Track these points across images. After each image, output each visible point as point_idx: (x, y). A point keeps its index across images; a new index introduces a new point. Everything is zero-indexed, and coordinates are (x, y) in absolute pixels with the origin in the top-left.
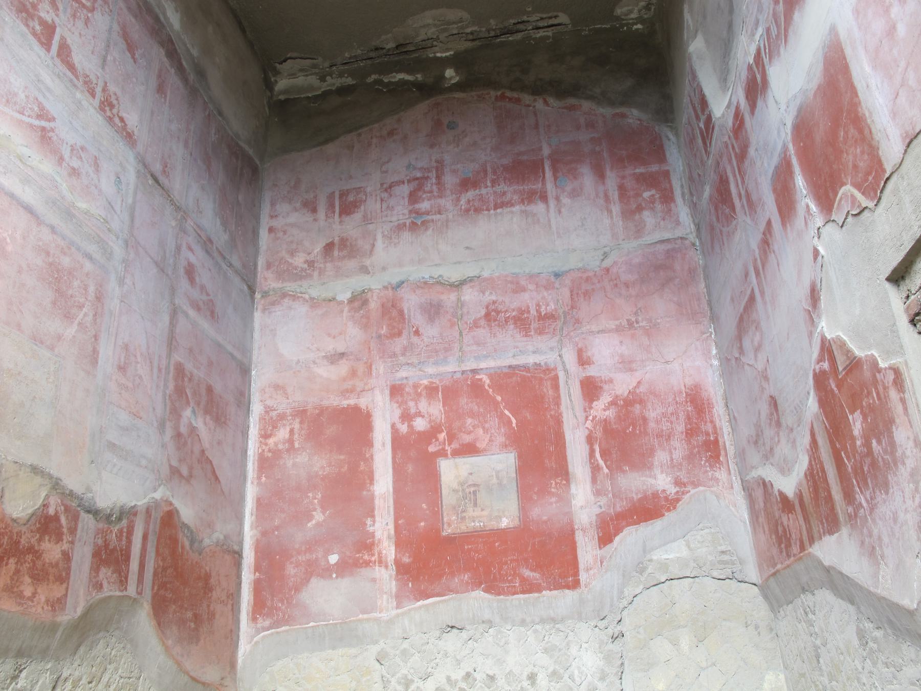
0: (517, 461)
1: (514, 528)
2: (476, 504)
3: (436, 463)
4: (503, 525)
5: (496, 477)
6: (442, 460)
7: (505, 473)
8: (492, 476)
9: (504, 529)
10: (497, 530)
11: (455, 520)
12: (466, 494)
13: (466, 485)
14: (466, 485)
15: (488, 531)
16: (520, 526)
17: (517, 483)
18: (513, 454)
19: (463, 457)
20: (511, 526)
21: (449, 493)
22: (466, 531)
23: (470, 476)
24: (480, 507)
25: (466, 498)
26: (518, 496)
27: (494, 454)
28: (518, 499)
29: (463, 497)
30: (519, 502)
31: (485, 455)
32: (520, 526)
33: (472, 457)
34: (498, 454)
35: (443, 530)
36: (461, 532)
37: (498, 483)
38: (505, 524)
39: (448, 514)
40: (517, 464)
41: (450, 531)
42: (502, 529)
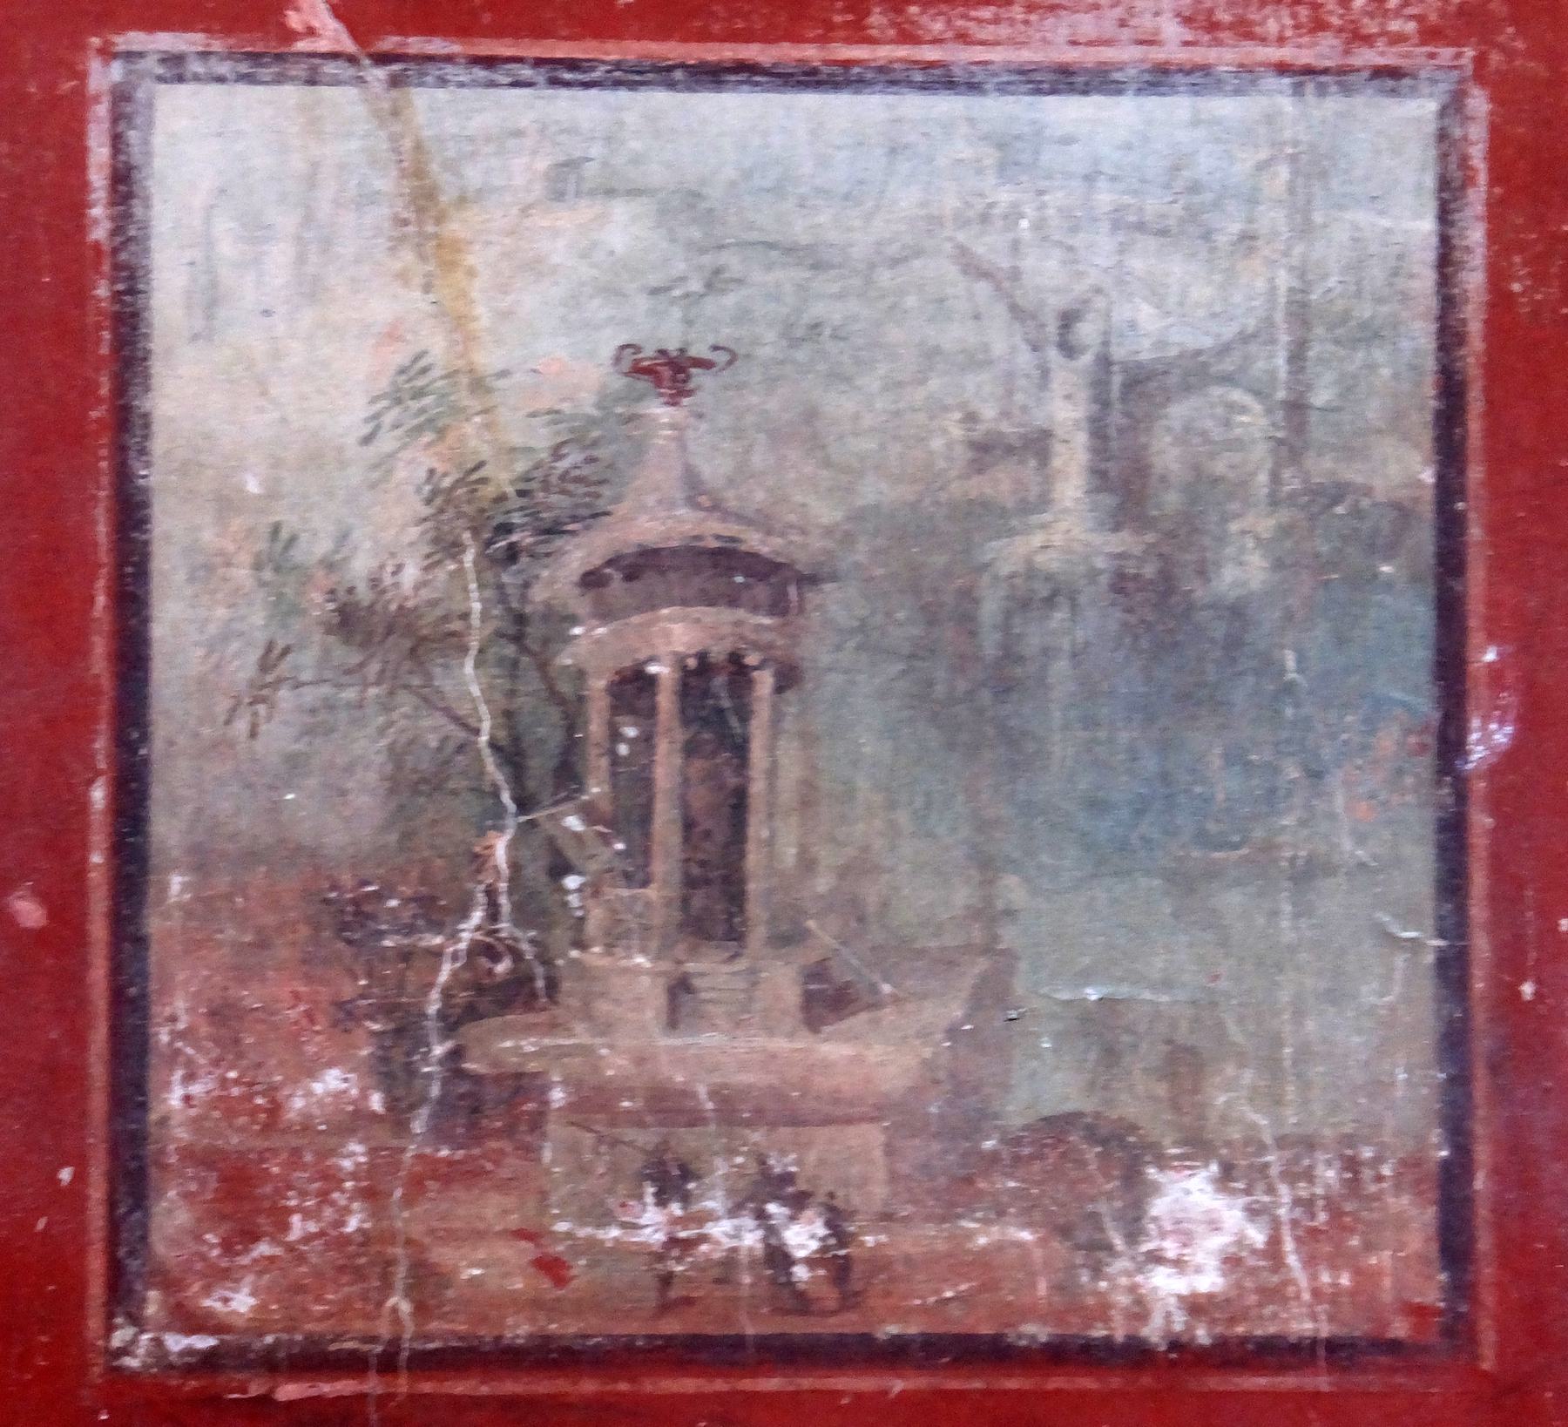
0: (1474, 235)
1: (1336, 1351)
2: (732, 888)
3: (75, 107)
4: (1165, 1284)
5: (1100, 478)
6: (175, 69)
7: (1255, 421)
8: (1038, 444)
9: (1182, 1352)
10: (1057, 1355)
11: (355, 1120)
12: (572, 712)
13: (579, 554)
14: (579, 554)
15: (895, 1354)
16: (1458, 1330)
17: (1449, 612)
18: (1421, 109)
19: (563, 73)
20: (1302, 1325)
21: (270, 659)
22: (519, 1330)
23: (659, 411)
24: (788, 938)
25: (568, 775)
26: (1452, 833)
27: (1100, 81)
28: (1452, 884)
29: (512, 754)
30: (1454, 926)
31: (941, 80)
32: (1458, 1330)
33: (711, 76)
34: (1159, 79)
35: (121, 1295)
36: (446, 1329)
37: (1122, 584)
38: (1209, 1281)
39: (223, 1015)
40: (1473, 279)
41: (242, 1302)
42: (1136, 1354)
